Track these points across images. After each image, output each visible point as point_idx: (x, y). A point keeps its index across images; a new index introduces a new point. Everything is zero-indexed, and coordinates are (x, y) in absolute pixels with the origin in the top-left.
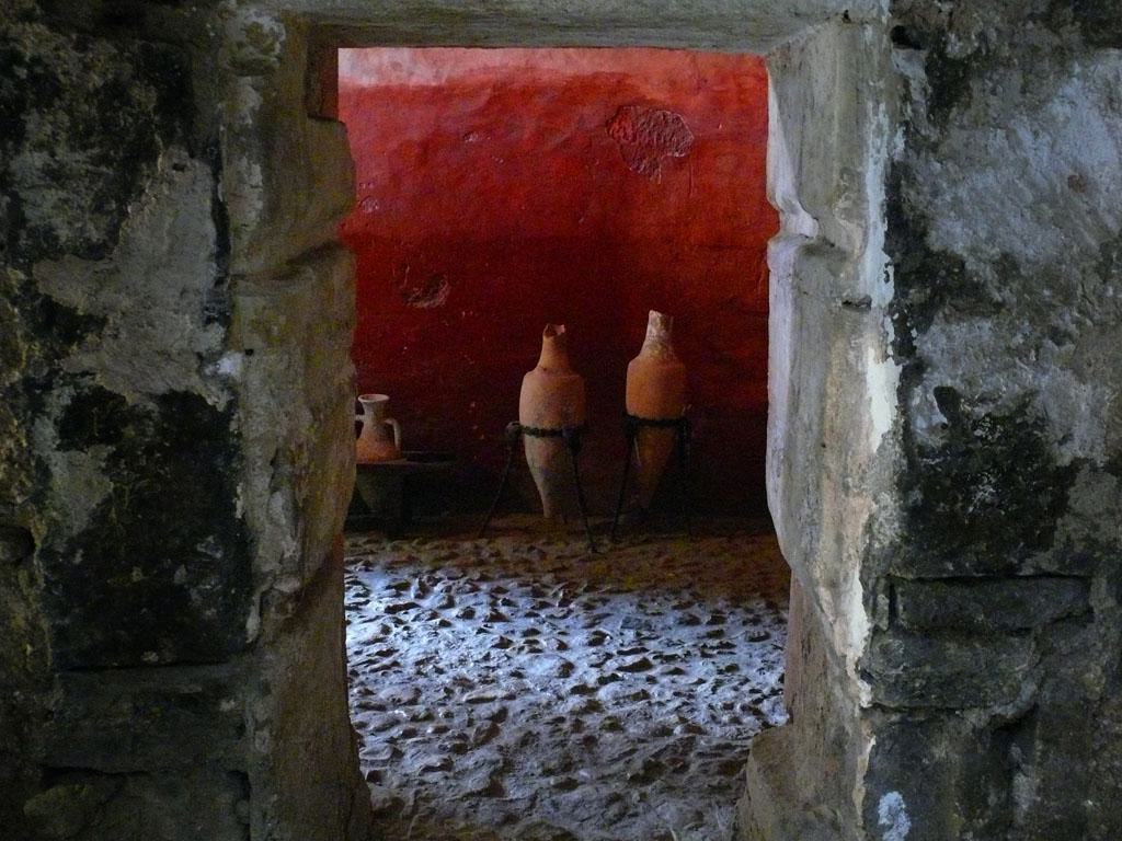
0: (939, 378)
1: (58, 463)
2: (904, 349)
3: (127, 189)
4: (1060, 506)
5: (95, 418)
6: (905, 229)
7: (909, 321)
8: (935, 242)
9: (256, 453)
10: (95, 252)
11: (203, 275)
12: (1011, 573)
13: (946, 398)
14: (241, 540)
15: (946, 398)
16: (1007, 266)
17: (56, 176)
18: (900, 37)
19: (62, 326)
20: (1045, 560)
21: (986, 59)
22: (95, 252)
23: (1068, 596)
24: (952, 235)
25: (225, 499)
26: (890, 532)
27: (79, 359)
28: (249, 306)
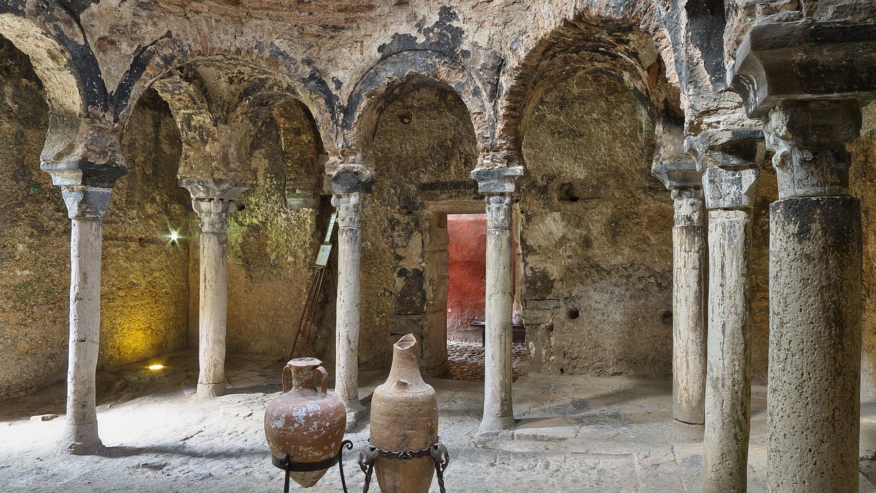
0: (530, 265)
1: (397, 280)
2: (524, 260)
3: (409, 238)
4: (552, 287)
5: (403, 273)
6: (523, 241)
7: (525, 255)
8: (528, 243)
9: (427, 279)
10: (405, 247)
11: (420, 251)
12: (544, 299)
13: (532, 268)
14: (424, 293)
15: (532, 268)
16: (540, 247)
17: (399, 236)
18: (522, 212)
19: (399, 258)
20: (550, 296)
21: (535, 214)
22: (405, 247)
23: (556, 303)
24: (530, 242)
25: (422, 285)
26: (525, 291)
27: (401, 263)
28: (426, 256)
